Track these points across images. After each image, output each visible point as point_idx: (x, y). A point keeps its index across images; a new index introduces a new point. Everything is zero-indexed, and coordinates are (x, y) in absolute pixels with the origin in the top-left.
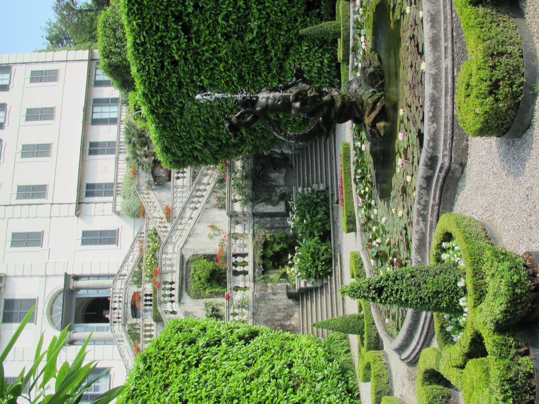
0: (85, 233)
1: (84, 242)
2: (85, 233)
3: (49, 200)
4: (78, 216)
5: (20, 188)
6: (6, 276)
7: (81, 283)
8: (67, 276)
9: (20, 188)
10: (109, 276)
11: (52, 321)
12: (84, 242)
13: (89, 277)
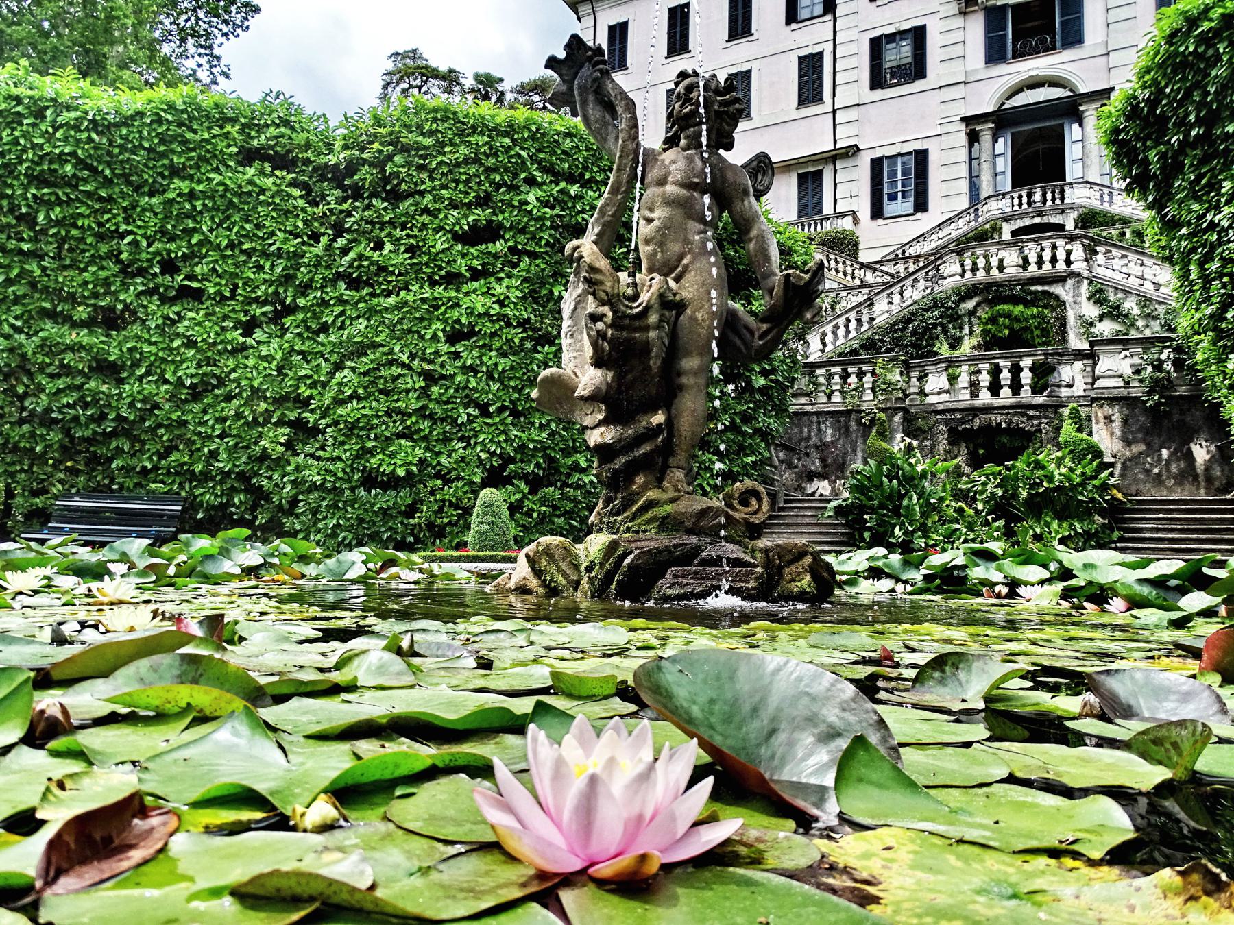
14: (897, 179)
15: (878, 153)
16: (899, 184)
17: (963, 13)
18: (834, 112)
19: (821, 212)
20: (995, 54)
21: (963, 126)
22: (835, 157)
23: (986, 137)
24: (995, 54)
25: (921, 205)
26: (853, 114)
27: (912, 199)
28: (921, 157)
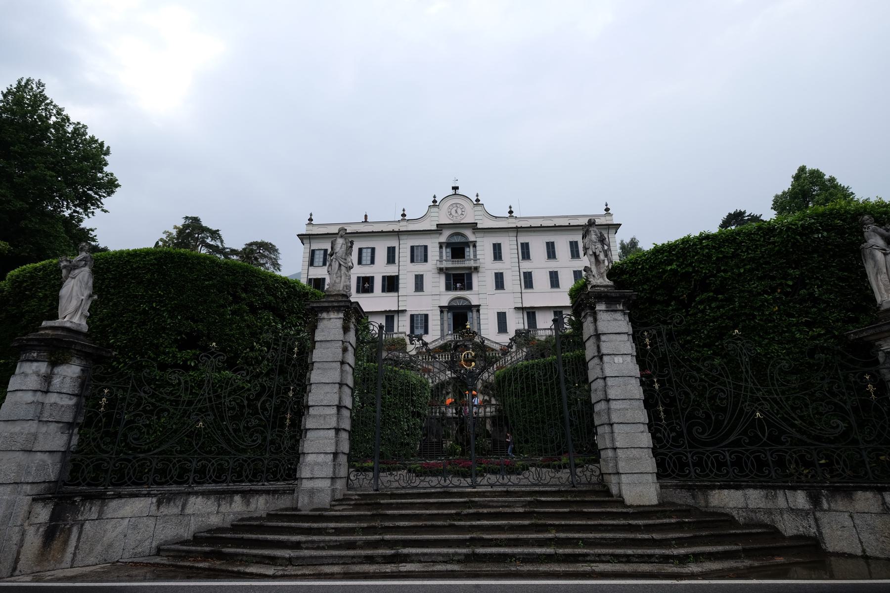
0: (505, 313)
2: (505, 313)
3: (523, 291)
5: (530, 273)
6: (478, 272)
7: (475, 314)
8: (479, 306)
9: (530, 273)
13: (479, 318)
14: (419, 323)
17: (439, 273)
18: (398, 296)
19: (393, 331)
23: (445, 313)
24: (448, 288)
26: (405, 298)
28: (426, 316)
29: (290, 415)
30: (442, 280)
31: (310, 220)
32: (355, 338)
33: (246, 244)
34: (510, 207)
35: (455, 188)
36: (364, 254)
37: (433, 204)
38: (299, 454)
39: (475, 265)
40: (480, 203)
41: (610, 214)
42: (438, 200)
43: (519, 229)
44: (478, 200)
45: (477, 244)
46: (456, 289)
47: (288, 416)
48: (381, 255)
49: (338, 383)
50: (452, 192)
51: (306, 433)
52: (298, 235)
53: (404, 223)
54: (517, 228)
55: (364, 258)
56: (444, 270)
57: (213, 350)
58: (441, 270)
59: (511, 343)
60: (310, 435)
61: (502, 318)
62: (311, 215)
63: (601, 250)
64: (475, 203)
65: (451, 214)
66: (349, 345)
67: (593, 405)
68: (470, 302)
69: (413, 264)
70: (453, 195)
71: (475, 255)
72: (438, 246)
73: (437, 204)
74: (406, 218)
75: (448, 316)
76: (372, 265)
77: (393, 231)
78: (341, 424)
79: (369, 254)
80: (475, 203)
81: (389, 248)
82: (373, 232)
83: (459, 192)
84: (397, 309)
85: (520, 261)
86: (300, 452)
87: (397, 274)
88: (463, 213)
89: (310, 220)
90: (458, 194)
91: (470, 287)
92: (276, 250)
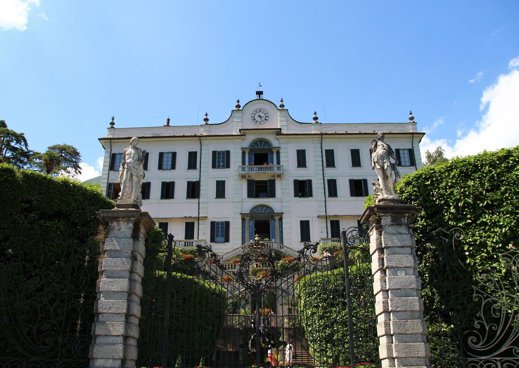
0: (308, 222)
1: (302, 223)
2: (308, 222)
4: (318, 217)
10: (282, 238)
11: (256, 207)
12: (302, 223)
15: (214, 220)
16: (220, 231)
20: (250, 195)
21: (240, 216)
22: (198, 218)
24: (250, 195)
25: (227, 240)
27: (224, 237)
29: (81, 321)
30: (244, 185)
31: (112, 124)
32: (144, 248)
33: (50, 148)
34: (315, 113)
35: (259, 93)
36: (165, 159)
37: (236, 109)
38: (89, 359)
39: (279, 172)
40: (284, 108)
41: (414, 122)
42: (242, 104)
43: (324, 136)
44: (282, 106)
45: (281, 151)
46: (257, 196)
47: (79, 322)
48: (182, 161)
49: (126, 292)
50: (256, 97)
51: (96, 338)
52: (99, 139)
53: (207, 128)
54: (322, 134)
55: (165, 163)
56: (247, 177)
57: (9, 256)
58: (243, 177)
59: (300, 255)
60: (98, 340)
61: (305, 226)
62: (113, 119)
63: (389, 165)
64: (279, 108)
65: (254, 119)
66: (139, 255)
67: (377, 316)
68: (272, 210)
69: (215, 169)
70: (257, 99)
71: (278, 162)
72: (240, 152)
73: (241, 109)
74: (209, 122)
75: (250, 225)
76: (173, 170)
77: (195, 136)
78: (129, 332)
79: (170, 159)
80: (279, 108)
81: (190, 153)
82: (174, 137)
83: (264, 96)
84: (197, 216)
85: (325, 168)
86: (90, 356)
87: (198, 180)
88: (267, 118)
89: (112, 124)
90: (262, 99)
91: (272, 195)
92: (78, 154)
